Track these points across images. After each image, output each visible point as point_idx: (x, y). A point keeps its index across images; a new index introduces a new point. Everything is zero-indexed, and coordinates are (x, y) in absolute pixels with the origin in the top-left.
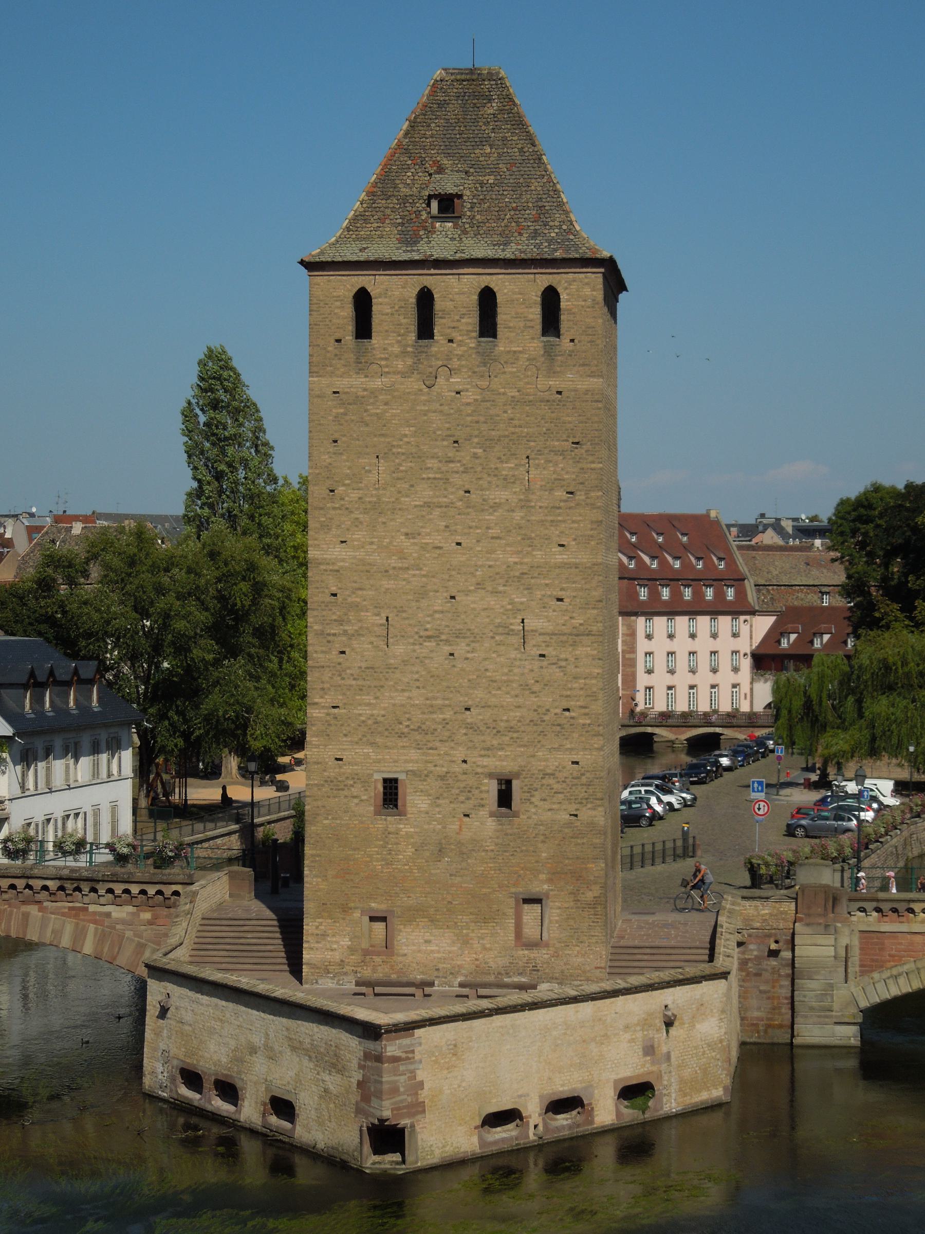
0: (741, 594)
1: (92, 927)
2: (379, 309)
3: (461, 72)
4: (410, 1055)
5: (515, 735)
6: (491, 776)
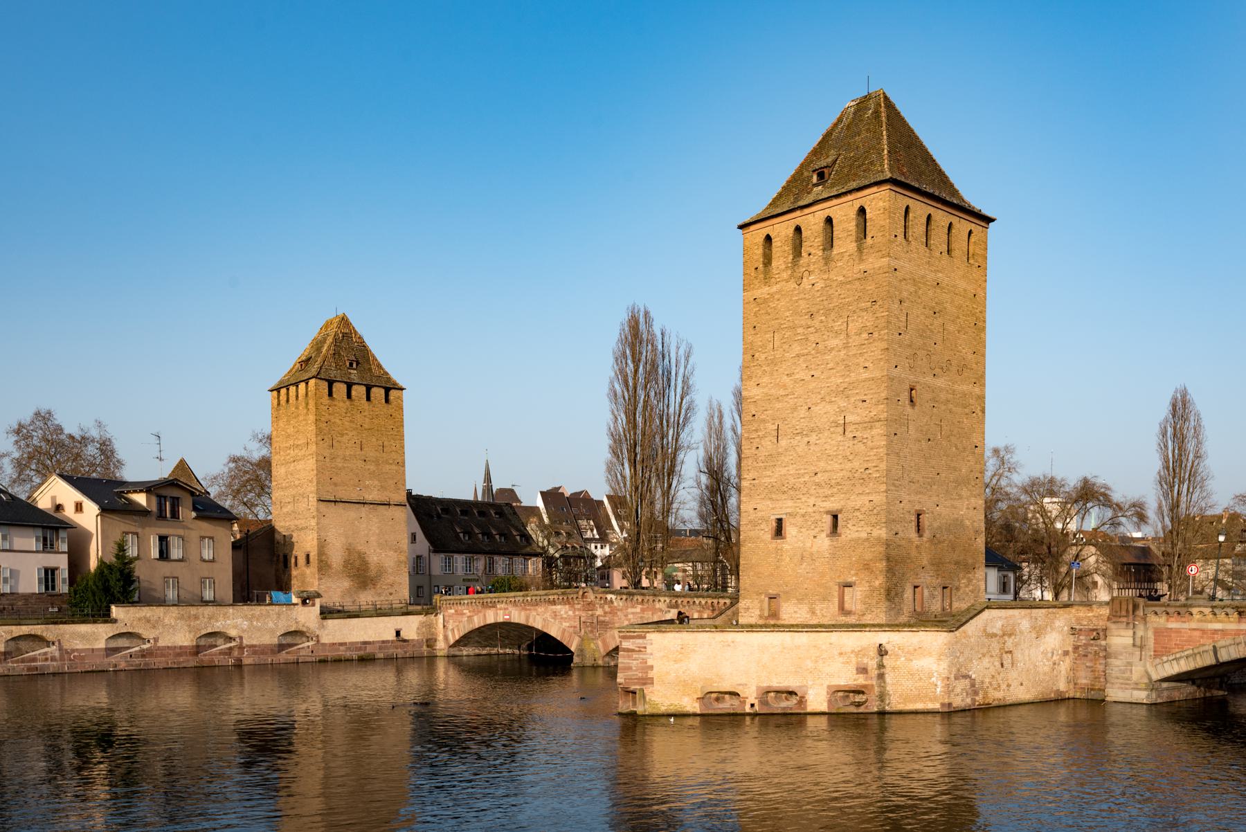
4: (642, 650)
5: (840, 487)
6: (827, 512)
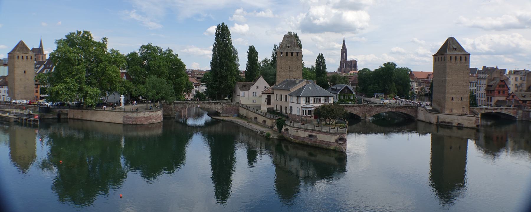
1: (406, 111)
2: (452, 58)
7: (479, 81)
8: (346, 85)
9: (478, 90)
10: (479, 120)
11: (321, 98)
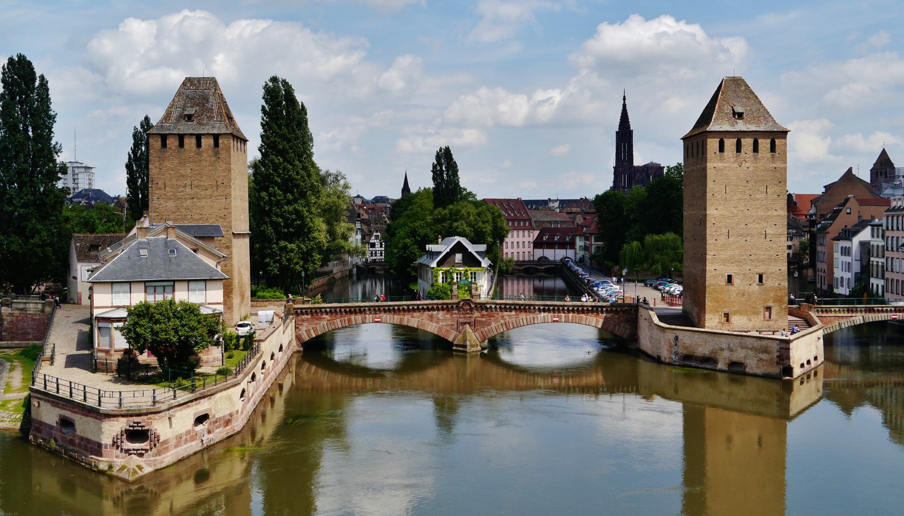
0: (530, 224)
3: (731, 77)
6: (757, 274)
7: (890, 218)
8: (458, 239)
9: (887, 250)
10: (789, 349)
11: (174, 286)
